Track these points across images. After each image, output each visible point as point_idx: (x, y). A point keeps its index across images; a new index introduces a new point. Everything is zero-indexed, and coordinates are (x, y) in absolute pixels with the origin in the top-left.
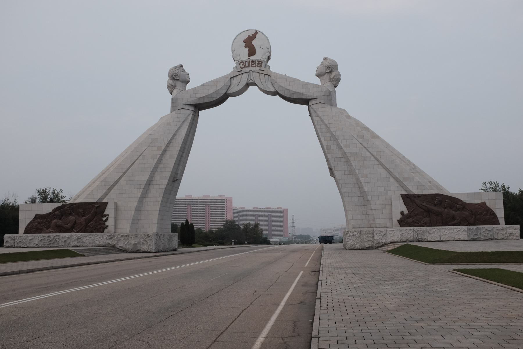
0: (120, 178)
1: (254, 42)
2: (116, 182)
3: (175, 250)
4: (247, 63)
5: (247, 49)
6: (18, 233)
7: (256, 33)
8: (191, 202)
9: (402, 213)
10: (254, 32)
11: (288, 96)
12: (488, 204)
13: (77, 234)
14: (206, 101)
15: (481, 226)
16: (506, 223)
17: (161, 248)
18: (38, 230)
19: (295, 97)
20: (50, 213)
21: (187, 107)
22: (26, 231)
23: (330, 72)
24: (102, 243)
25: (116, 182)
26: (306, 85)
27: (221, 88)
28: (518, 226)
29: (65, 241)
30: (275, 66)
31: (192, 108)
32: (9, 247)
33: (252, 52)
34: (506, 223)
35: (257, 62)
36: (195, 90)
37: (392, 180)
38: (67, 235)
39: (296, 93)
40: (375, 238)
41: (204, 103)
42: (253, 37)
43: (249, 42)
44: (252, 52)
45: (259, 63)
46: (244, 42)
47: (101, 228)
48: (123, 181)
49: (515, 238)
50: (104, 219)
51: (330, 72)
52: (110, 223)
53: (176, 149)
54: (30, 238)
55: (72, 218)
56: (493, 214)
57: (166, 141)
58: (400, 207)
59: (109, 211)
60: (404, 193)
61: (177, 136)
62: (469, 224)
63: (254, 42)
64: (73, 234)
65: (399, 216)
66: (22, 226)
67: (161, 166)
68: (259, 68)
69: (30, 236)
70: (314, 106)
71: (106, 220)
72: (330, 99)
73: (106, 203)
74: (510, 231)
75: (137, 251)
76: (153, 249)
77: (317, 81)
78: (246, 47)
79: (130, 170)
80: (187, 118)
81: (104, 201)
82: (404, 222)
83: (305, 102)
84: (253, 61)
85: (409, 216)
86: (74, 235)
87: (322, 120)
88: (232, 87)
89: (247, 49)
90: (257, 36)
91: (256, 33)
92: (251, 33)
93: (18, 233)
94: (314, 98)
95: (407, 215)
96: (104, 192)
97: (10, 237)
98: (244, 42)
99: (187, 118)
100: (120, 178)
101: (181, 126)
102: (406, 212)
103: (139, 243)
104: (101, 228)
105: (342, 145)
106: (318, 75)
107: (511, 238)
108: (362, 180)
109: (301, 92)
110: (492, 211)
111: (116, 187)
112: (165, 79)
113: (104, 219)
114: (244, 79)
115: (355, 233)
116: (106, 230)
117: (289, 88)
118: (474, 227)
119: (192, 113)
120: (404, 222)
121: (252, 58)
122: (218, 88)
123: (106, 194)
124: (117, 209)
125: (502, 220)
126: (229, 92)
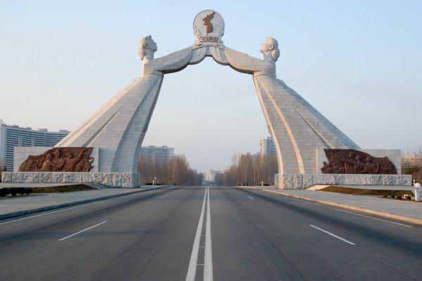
2: (99, 131)
7: (214, 13)
8: (151, 149)
9: (325, 163)
11: (238, 68)
13: (68, 173)
14: (172, 68)
15: (383, 175)
16: (403, 173)
18: (31, 169)
20: (42, 156)
21: (158, 73)
22: (23, 169)
23: (274, 49)
24: (90, 180)
25: (99, 131)
26: (254, 59)
29: (57, 179)
30: (227, 40)
31: (161, 73)
32: (7, 182)
34: (403, 173)
36: (164, 59)
37: (317, 138)
38: (60, 173)
40: (304, 180)
43: (209, 20)
44: (210, 29)
45: (216, 40)
50: (90, 161)
51: (274, 49)
52: (95, 164)
53: (141, 107)
55: (61, 160)
57: (140, 100)
58: (320, 159)
59: (95, 155)
60: (326, 148)
62: (374, 173)
63: (213, 21)
65: (322, 166)
67: (136, 119)
69: (27, 173)
71: (92, 162)
72: (271, 72)
73: (92, 149)
76: (131, 185)
77: (261, 57)
82: (323, 170)
83: (251, 73)
85: (330, 165)
86: (65, 174)
88: (193, 57)
92: (209, 13)
99: (156, 82)
103: (121, 181)
110: (392, 164)
112: (138, 45)
113: (90, 161)
118: (378, 175)
121: (211, 35)
124: (100, 151)
126: (191, 61)
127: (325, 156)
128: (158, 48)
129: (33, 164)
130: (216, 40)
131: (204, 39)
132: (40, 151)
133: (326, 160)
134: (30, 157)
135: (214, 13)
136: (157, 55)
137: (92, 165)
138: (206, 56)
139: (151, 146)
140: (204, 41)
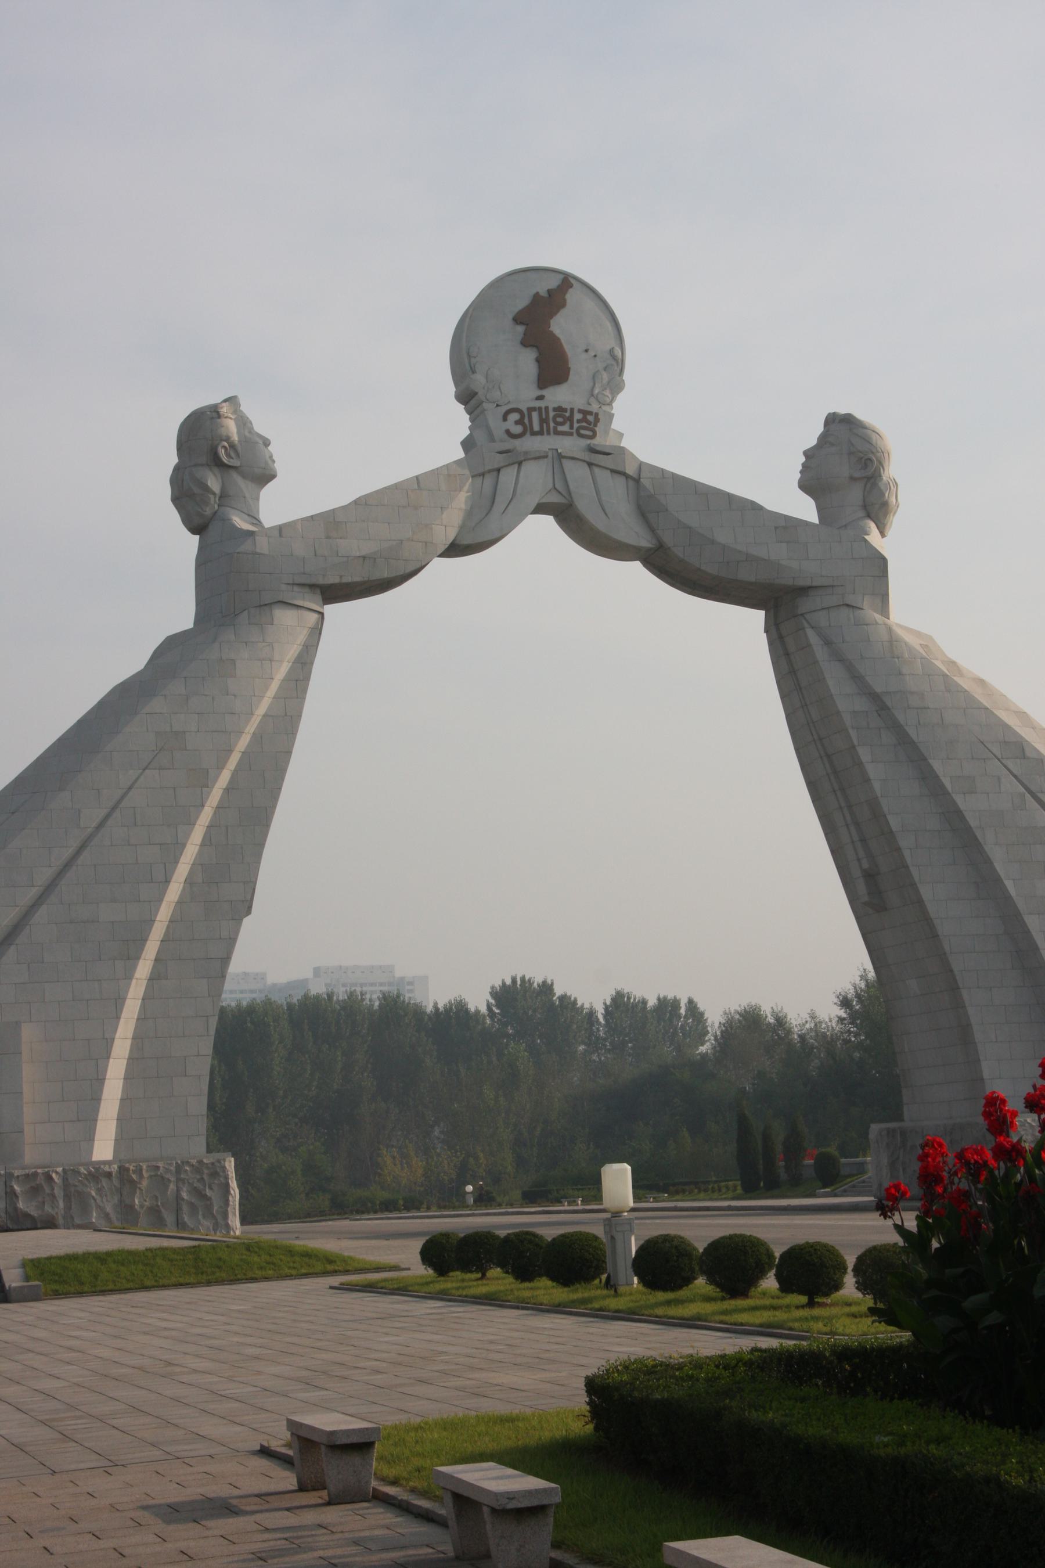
4: (535, 415)
19: (746, 574)
33: (553, 368)
35: (578, 416)
36: (330, 522)
46: (517, 320)
68: (584, 443)
78: (525, 343)
84: (559, 409)
87: (857, 678)
94: (798, 575)
98: (517, 320)
105: (947, 783)
106: (807, 486)
108: (1032, 922)
117: (722, 537)
121: (559, 396)
126: (467, 541)
128: (279, 467)
130: (588, 422)
135: (567, 281)
136: (277, 506)
138: (541, 509)
139: (667, 1007)
140: (527, 430)
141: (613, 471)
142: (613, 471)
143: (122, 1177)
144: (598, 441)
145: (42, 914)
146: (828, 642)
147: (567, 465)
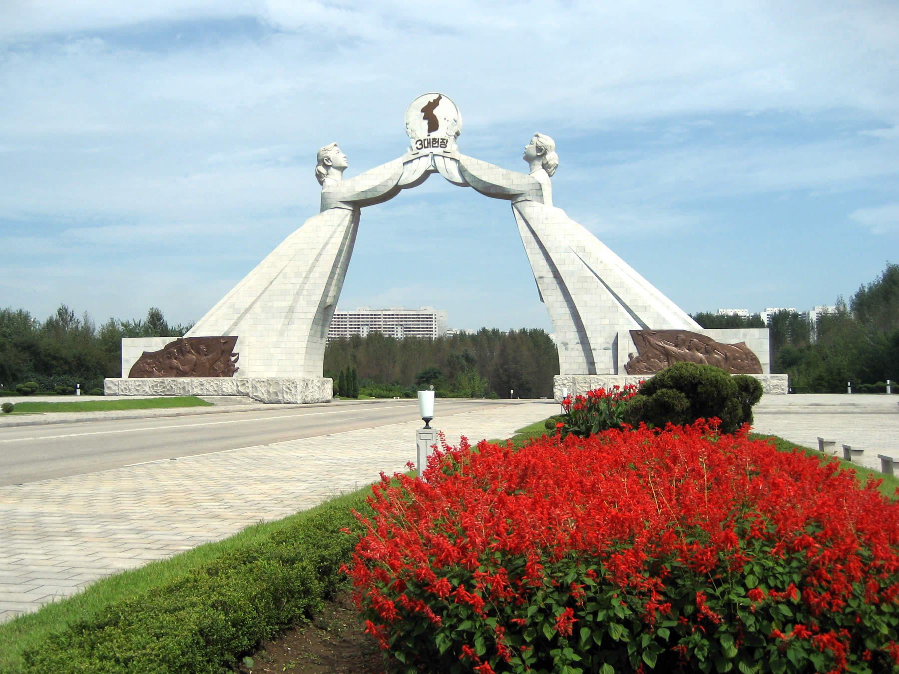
0: (253, 304)
1: (436, 112)
2: (247, 310)
3: (328, 401)
5: (426, 122)
6: (120, 376)
9: (630, 355)
10: (436, 97)
12: (748, 345)
14: (370, 196)
17: (309, 399)
19: (492, 191)
21: (343, 206)
27: (391, 179)
28: (786, 376)
33: (433, 125)
39: (493, 185)
41: (366, 200)
42: (435, 103)
44: (433, 125)
45: (444, 143)
46: (422, 111)
47: (229, 370)
48: (257, 308)
49: (779, 391)
50: (233, 359)
54: (138, 383)
56: (755, 359)
58: (628, 348)
61: (329, 246)
63: (436, 112)
64: (193, 379)
66: (126, 369)
70: (518, 205)
71: (236, 361)
74: (775, 382)
75: (278, 402)
78: (424, 118)
79: (267, 293)
80: (343, 220)
81: (231, 335)
82: (631, 368)
84: (434, 139)
89: (426, 122)
90: (440, 102)
91: (440, 98)
92: (432, 98)
93: (120, 376)
95: (637, 358)
96: (232, 322)
97: (112, 382)
98: (422, 111)
99: (343, 220)
100: (253, 304)
101: (335, 232)
102: (636, 354)
104: (229, 370)
107: (774, 391)
109: (500, 185)
111: (248, 316)
113: (233, 359)
114: (423, 165)
115: (565, 382)
116: (235, 374)
117: (484, 179)
119: (350, 213)
120: (631, 368)
121: (434, 135)
122: (386, 178)
123: (236, 324)
125: (767, 369)
126: (401, 183)
127: (631, 342)
129: (146, 367)
131: (422, 142)
132: (157, 344)
133: (633, 350)
134: (144, 353)
137: (237, 365)
140: (423, 146)
141: (451, 159)
142: (451, 159)
143: (269, 382)
144: (446, 150)
145: (258, 305)
146: (520, 213)
147: (436, 158)
